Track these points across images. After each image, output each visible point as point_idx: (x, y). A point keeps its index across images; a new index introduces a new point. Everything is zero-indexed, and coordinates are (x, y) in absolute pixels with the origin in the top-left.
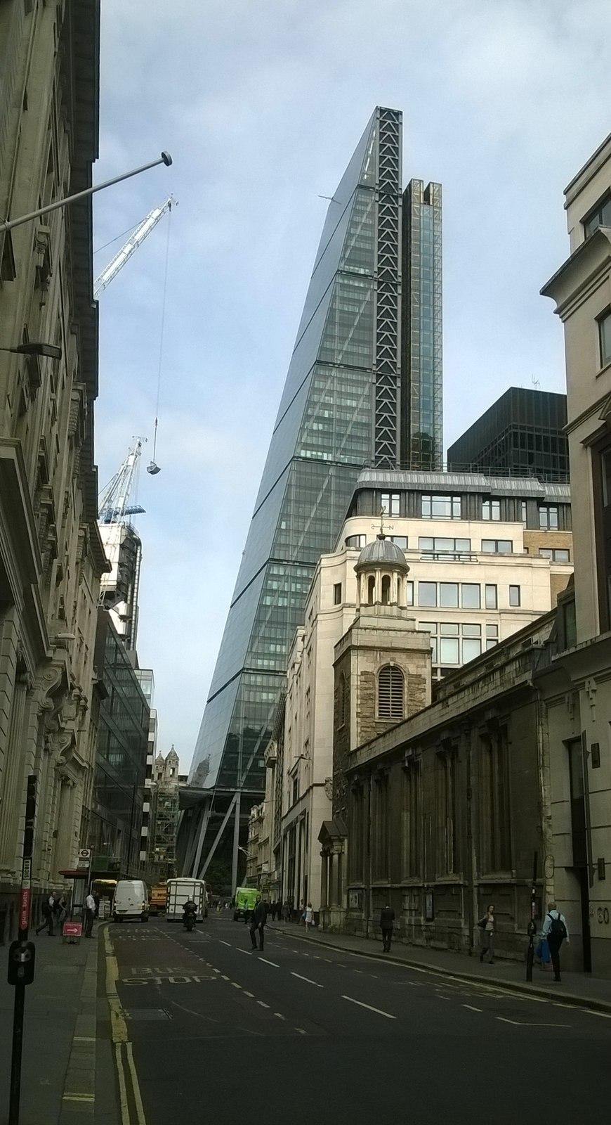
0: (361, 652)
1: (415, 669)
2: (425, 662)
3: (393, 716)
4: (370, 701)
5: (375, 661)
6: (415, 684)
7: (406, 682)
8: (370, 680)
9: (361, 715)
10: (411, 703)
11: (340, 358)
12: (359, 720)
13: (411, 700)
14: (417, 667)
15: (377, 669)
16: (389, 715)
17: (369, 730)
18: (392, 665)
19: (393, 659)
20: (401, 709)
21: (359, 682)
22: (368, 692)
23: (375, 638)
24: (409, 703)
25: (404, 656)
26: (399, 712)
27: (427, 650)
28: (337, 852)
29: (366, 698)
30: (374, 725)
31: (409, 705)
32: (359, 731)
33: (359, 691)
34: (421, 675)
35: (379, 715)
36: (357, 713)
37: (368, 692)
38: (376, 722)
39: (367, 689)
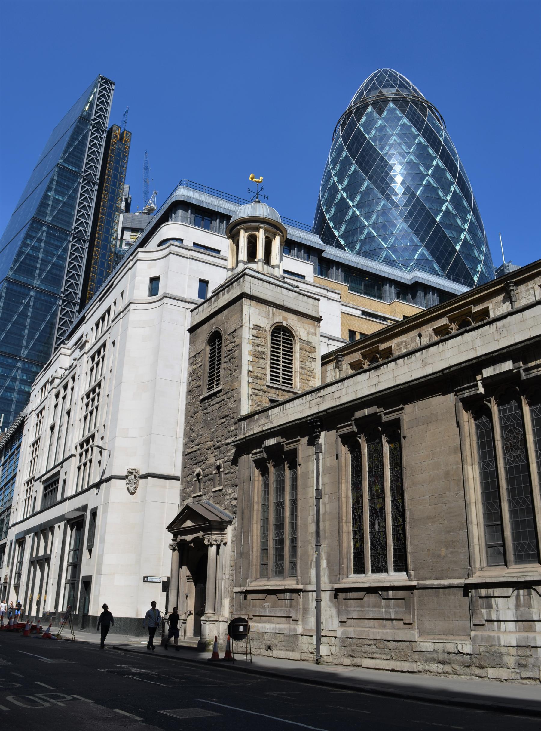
0: (253, 303)
1: (306, 335)
2: (315, 330)
3: (283, 382)
4: (261, 361)
5: (267, 316)
6: (306, 351)
7: (297, 348)
8: (262, 336)
9: (252, 374)
10: (303, 371)
11: (50, 219)
12: (251, 380)
13: (302, 368)
14: (308, 333)
15: (269, 326)
16: (279, 381)
17: (260, 393)
18: (284, 324)
19: (285, 319)
20: (291, 376)
21: (251, 336)
22: (260, 349)
23: (268, 292)
24: (301, 370)
25: (295, 318)
26: (288, 380)
27: (317, 318)
28: (215, 543)
29: (259, 356)
30: (265, 388)
31: (301, 373)
32: (250, 393)
33: (251, 346)
34: (310, 342)
35: (271, 379)
36: (249, 371)
37: (260, 349)
38: (268, 386)
39: (259, 345)
